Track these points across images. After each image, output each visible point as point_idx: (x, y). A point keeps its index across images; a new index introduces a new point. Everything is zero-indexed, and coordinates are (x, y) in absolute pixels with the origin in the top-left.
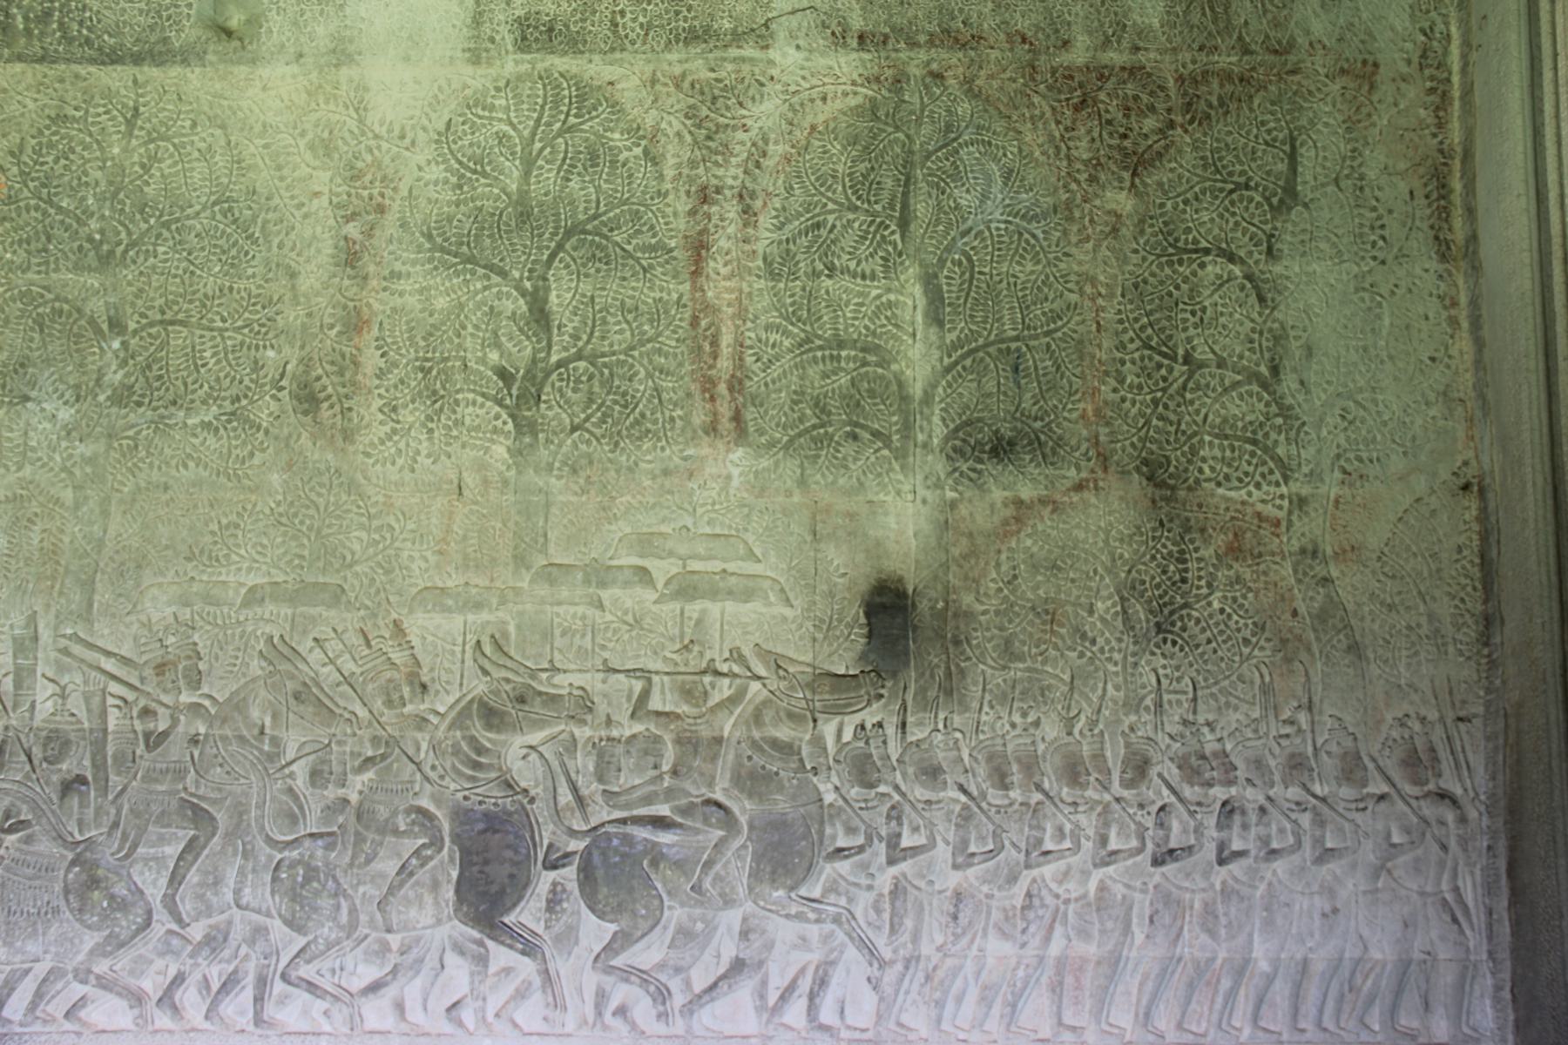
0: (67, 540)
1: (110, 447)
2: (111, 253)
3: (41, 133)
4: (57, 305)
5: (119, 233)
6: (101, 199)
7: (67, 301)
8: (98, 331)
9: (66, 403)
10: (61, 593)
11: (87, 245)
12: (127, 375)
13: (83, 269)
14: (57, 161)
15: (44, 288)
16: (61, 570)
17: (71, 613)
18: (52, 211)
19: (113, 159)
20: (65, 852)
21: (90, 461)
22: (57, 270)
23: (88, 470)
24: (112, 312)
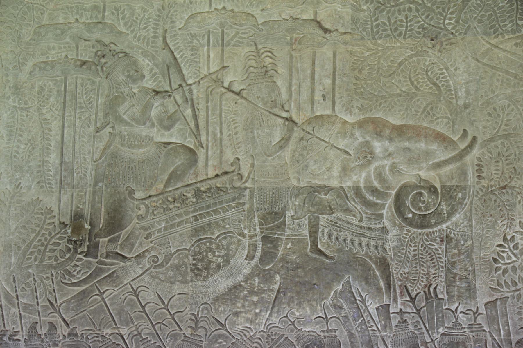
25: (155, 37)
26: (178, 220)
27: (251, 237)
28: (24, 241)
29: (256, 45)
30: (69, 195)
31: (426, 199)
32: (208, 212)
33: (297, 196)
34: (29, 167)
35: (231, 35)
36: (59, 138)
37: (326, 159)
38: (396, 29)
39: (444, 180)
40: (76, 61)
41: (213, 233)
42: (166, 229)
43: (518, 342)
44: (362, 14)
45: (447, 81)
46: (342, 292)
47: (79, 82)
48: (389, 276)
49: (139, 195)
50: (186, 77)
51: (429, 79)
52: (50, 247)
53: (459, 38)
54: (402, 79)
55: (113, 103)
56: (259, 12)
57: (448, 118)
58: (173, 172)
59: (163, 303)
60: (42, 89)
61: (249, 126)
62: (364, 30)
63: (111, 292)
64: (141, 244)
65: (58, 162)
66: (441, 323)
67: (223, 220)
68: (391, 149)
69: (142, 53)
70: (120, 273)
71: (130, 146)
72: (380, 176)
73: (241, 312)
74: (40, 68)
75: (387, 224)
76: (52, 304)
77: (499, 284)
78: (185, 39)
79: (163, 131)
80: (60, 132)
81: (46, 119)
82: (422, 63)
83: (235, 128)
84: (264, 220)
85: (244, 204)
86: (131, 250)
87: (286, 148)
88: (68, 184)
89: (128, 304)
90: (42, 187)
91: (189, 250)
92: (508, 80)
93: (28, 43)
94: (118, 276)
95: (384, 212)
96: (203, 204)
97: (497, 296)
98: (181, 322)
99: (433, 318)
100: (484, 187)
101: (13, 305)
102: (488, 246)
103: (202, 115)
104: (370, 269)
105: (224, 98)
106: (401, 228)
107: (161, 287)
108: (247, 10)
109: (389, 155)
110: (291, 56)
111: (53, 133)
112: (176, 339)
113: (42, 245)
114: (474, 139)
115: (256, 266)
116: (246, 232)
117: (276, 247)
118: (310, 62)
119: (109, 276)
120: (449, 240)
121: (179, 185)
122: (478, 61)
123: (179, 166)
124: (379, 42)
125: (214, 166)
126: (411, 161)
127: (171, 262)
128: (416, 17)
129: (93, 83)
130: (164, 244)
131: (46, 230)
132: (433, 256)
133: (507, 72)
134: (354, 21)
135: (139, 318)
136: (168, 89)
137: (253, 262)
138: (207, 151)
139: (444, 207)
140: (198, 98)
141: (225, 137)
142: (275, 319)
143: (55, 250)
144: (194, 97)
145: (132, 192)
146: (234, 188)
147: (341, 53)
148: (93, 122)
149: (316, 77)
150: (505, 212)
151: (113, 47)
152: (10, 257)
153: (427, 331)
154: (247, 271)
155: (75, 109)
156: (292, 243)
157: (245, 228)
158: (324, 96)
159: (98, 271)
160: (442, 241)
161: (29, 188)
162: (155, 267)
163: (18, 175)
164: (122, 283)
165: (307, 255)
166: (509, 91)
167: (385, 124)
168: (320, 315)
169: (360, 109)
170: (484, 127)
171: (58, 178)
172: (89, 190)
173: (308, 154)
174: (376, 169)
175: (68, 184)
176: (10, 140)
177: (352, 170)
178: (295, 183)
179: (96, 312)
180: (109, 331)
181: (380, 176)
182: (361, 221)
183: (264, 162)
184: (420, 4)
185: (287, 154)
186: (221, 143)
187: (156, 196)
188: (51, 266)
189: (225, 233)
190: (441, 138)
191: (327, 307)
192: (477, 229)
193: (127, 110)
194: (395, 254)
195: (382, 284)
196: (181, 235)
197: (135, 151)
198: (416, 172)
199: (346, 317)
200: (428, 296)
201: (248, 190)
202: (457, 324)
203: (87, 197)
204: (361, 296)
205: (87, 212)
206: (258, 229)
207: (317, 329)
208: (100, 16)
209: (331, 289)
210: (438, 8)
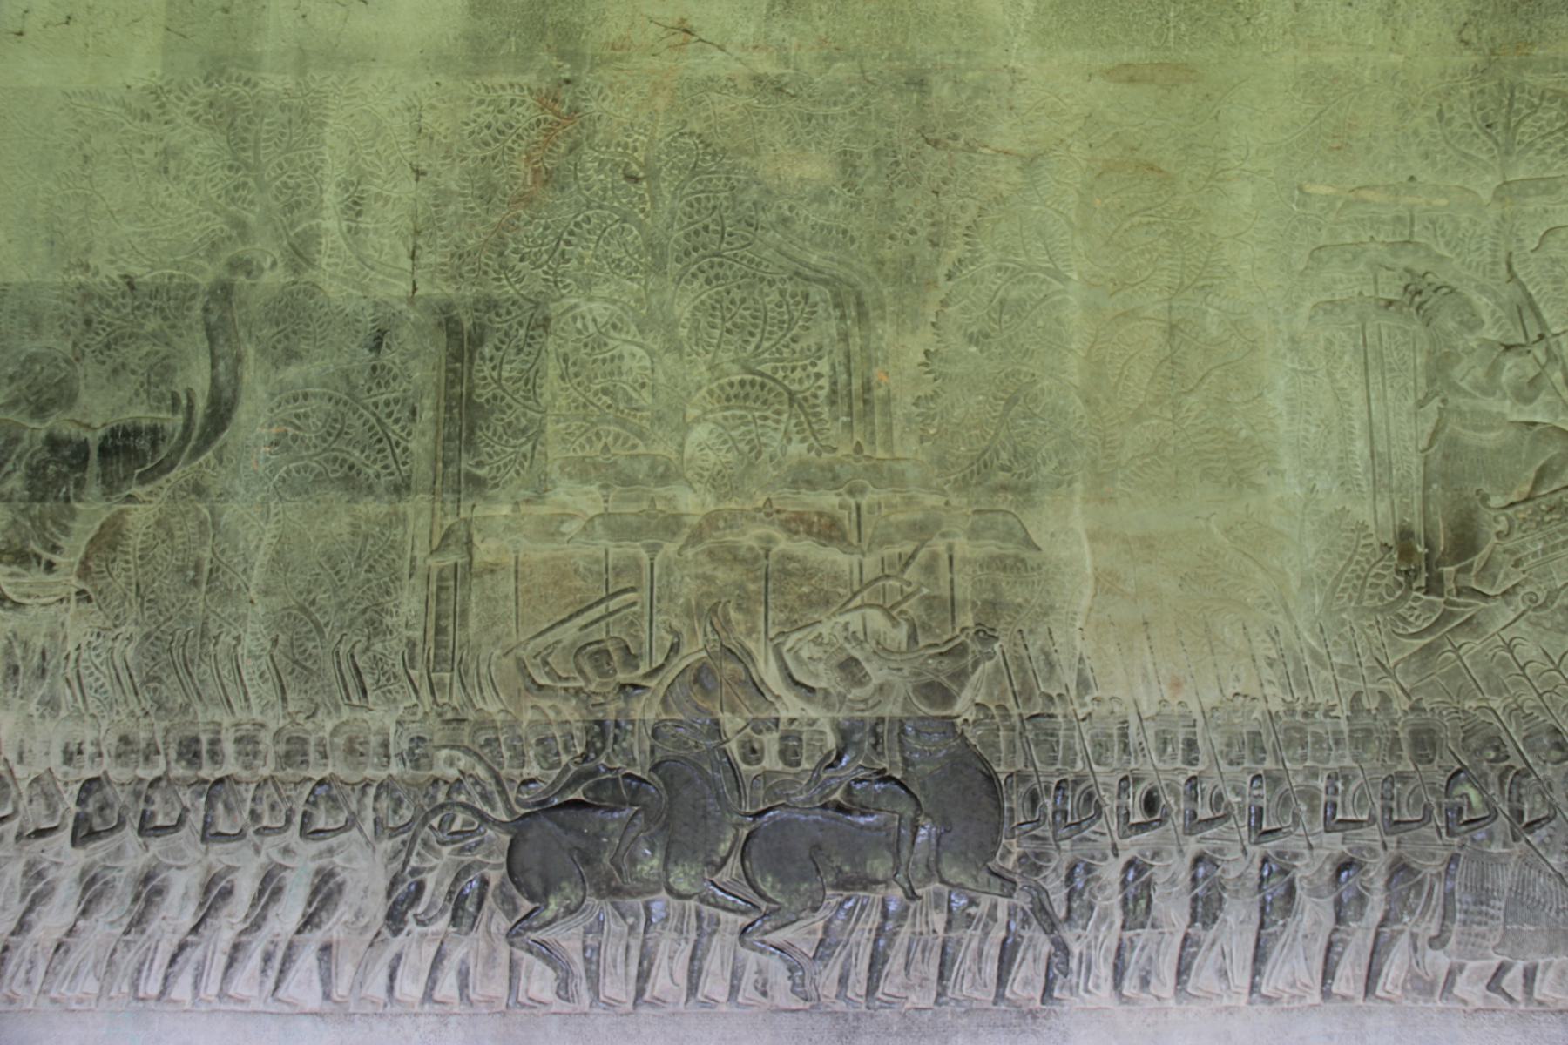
25: (1494, 263)
30: (1387, 501)
36: (1365, 416)
42: (1544, 551)
47: (1384, 331)
49: (1496, 501)
52: (1370, 580)
60: (1329, 342)
63: (1471, 646)
64: (1507, 576)
65: (1367, 452)
71: (1476, 428)
79: (1520, 406)
80: (1365, 408)
81: (1342, 389)
86: (1494, 584)
89: (1499, 664)
90: (1348, 491)
93: (1302, 273)
94: (1479, 624)
101: (1324, 666)
107: (1545, 639)
111: (1355, 409)
113: (1358, 577)
119: (1468, 622)
121: (1556, 486)
127: (1558, 601)
129: (1406, 332)
131: (1362, 554)
135: (1516, 684)
136: (1523, 341)
143: (1378, 585)
145: (1485, 499)
148: (1412, 393)
152: (1313, 595)
155: (1383, 373)
159: (1446, 617)
161: (1329, 492)
162: (1535, 609)
163: (1310, 473)
171: (1370, 476)
179: (1448, 676)
180: (1474, 704)
188: (1375, 609)
193: (1467, 372)
197: (1484, 435)
205: (1418, 528)
208: (1407, 232)
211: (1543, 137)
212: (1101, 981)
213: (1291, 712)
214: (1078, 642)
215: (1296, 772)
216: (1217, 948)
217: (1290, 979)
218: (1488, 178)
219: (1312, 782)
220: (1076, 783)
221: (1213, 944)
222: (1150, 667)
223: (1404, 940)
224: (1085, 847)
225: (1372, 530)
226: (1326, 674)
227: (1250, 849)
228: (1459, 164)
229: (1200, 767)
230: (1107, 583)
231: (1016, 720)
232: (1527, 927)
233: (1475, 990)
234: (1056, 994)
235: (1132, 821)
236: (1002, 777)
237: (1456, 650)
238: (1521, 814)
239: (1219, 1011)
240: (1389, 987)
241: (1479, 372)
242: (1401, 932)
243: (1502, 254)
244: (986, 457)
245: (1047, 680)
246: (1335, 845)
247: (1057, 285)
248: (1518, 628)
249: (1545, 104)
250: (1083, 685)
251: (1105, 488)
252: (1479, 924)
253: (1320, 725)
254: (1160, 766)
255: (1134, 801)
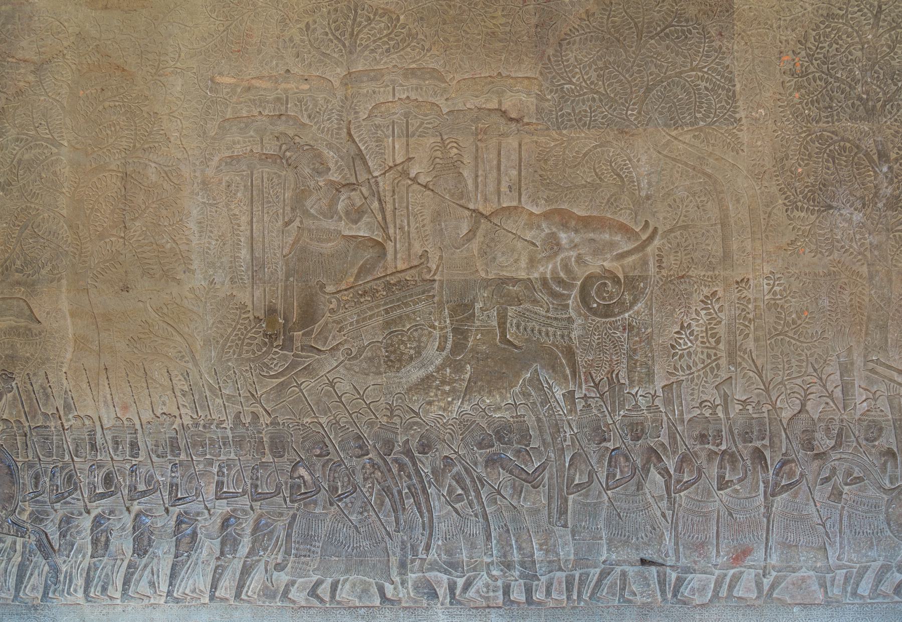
0: (867, 299)
1: (888, 238)
2: (874, 107)
3: (818, 27)
4: (842, 144)
5: (878, 93)
6: (863, 71)
7: (849, 141)
8: (871, 161)
9: (856, 210)
10: (867, 334)
11: (857, 103)
12: (894, 190)
13: (856, 119)
14: (830, 46)
15: (833, 133)
16: (865, 318)
17: (876, 346)
18: (830, 80)
19: (868, 42)
20: (884, 496)
21: (877, 247)
22: (839, 120)
23: (876, 253)
24: (880, 147)
25: (339, 129)
26: (369, 313)
27: (442, 329)
28: (222, 336)
29: (441, 135)
30: (262, 289)
31: (610, 289)
32: (399, 306)
33: (485, 288)
34: (221, 263)
35: (416, 125)
36: (248, 233)
37: (513, 251)
38: (580, 119)
39: (627, 270)
40: (261, 155)
41: (404, 326)
42: (358, 322)
43: (690, 420)
44: (547, 104)
45: (630, 172)
46: (530, 380)
47: (265, 176)
48: (574, 364)
49: (330, 289)
50: (371, 169)
51: (613, 170)
52: (246, 341)
53: (641, 129)
54: (587, 170)
55: (301, 196)
56: (443, 101)
57: (631, 209)
58: (362, 265)
59: (359, 393)
61: (437, 217)
62: (549, 120)
64: (334, 337)
65: (248, 257)
66: (622, 406)
67: (414, 313)
68: (577, 240)
69: (327, 145)
70: (315, 365)
71: (319, 240)
72: (566, 267)
73: (434, 401)
74: (226, 163)
75: (573, 314)
76: (253, 395)
77: (675, 369)
78: (369, 130)
80: (249, 227)
81: (235, 215)
82: (606, 154)
83: (423, 220)
84: (454, 312)
85: (434, 296)
87: (474, 241)
88: (260, 279)
89: (325, 395)
91: (381, 343)
92: (687, 171)
93: (213, 138)
94: (314, 369)
95: (570, 302)
96: (393, 297)
97: (674, 379)
98: (377, 411)
99: (615, 402)
100: (663, 276)
101: (217, 396)
102: (666, 332)
103: (389, 208)
104: (557, 357)
105: (410, 189)
106: (586, 318)
107: (355, 378)
108: (430, 99)
109: (575, 246)
110: (477, 146)
111: (242, 228)
112: (372, 428)
114: (656, 229)
115: (447, 357)
116: (436, 324)
117: (466, 339)
118: (496, 152)
119: (305, 368)
120: (631, 327)
121: (369, 278)
122: (660, 153)
123: (368, 260)
124: (564, 132)
125: (403, 259)
126: (596, 253)
128: (600, 107)
129: (280, 176)
130: (357, 337)
132: (616, 343)
133: (686, 164)
134: (539, 111)
136: (353, 180)
137: (444, 353)
138: (395, 244)
139: (627, 297)
140: (384, 190)
141: (413, 230)
142: (467, 407)
144: (381, 190)
145: (323, 286)
146: (423, 280)
147: (526, 143)
148: (281, 217)
149: (502, 168)
150: (683, 300)
151: (297, 140)
153: (610, 413)
154: (438, 362)
156: (482, 334)
157: (435, 320)
158: (510, 187)
159: (293, 365)
160: (624, 329)
161: (223, 284)
162: (349, 360)
164: (318, 375)
165: (496, 345)
166: (688, 183)
167: (571, 215)
168: (510, 402)
169: (546, 200)
170: (665, 218)
171: (250, 273)
172: (281, 284)
173: (496, 246)
174: (562, 260)
175: (260, 279)
176: (201, 236)
177: (539, 262)
178: (483, 275)
181: (566, 267)
182: (548, 311)
183: (453, 254)
184: (603, 95)
185: (475, 246)
186: (409, 235)
187: (346, 290)
188: (249, 360)
189: (416, 326)
190: (624, 229)
191: (516, 394)
192: (656, 318)
194: (580, 343)
195: (568, 372)
196: (373, 328)
197: (324, 245)
198: (600, 263)
199: (534, 403)
200: (610, 382)
201: (437, 283)
202: (636, 407)
203: (279, 291)
204: (548, 383)
205: (280, 307)
206: (448, 321)
207: (507, 415)
209: (520, 377)
210: (621, 98)
211: (375, 41)
212: (78, 588)
213: (197, 425)
214: (65, 382)
215: (199, 462)
216: (149, 569)
217: (192, 587)
218: (339, 70)
219: (209, 469)
220: (62, 468)
221: (146, 566)
222: (109, 396)
223: (262, 565)
224: (68, 508)
225: (250, 308)
226: (219, 401)
227: (171, 509)
228: (320, 61)
229: (140, 459)
230: (81, 342)
231: (27, 429)
232: (334, 558)
233: (301, 595)
234: (50, 595)
235: (97, 491)
236: (19, 464)
237: (299, 386)
238: (337, 489)
239: (147, 606)
240: (250, 593)
241: (325, 202)
242: (259, 561)
243: (344, 124)
244: (7, 263)
245: (45, 405)
246: (223, 508)
247: (55, 150)
248: (339, 372)
249: (377, 18)
250: (68, 407)
251: (81, 283)
252: (305, 556)
253: (214, 433)
254: (115, 458)
255: (98, 479)
